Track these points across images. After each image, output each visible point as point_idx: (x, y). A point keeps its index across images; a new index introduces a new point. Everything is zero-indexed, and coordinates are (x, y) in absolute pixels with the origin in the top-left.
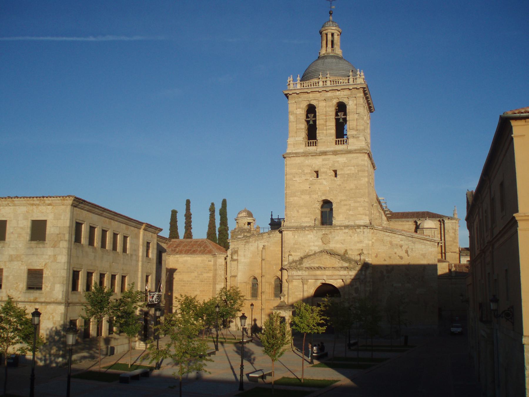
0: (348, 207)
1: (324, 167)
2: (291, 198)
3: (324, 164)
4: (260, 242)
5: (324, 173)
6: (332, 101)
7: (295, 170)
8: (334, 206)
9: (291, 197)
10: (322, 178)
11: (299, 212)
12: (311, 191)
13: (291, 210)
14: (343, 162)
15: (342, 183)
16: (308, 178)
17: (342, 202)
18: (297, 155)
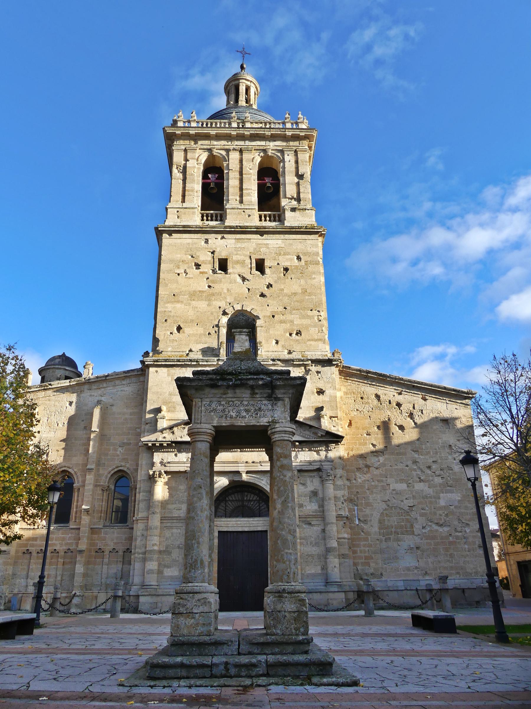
0: (288, 326)
1: (238, 252)
2: (169, 305)
3: (240, 247)
4: (91, 396)
5: (237, 262)
6: (254, 155)
7: (179, 256)
8: (258, 323)
9: (168, 303)
10: (235, 271)
11: (184, 332)
12: (213, 294)
13: (168, 328)
14: (278, 246)
15: (276, 282)
16: (206, 270)
17: (276, 316)
18: (186, 230)
